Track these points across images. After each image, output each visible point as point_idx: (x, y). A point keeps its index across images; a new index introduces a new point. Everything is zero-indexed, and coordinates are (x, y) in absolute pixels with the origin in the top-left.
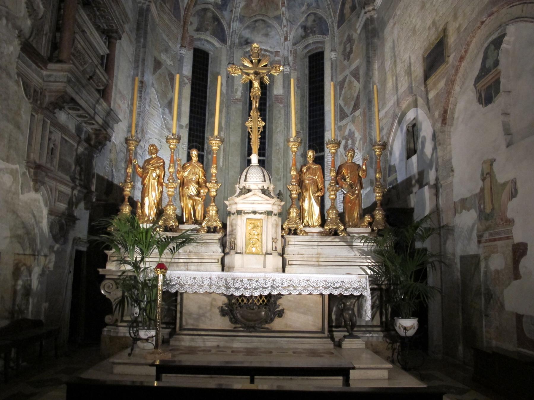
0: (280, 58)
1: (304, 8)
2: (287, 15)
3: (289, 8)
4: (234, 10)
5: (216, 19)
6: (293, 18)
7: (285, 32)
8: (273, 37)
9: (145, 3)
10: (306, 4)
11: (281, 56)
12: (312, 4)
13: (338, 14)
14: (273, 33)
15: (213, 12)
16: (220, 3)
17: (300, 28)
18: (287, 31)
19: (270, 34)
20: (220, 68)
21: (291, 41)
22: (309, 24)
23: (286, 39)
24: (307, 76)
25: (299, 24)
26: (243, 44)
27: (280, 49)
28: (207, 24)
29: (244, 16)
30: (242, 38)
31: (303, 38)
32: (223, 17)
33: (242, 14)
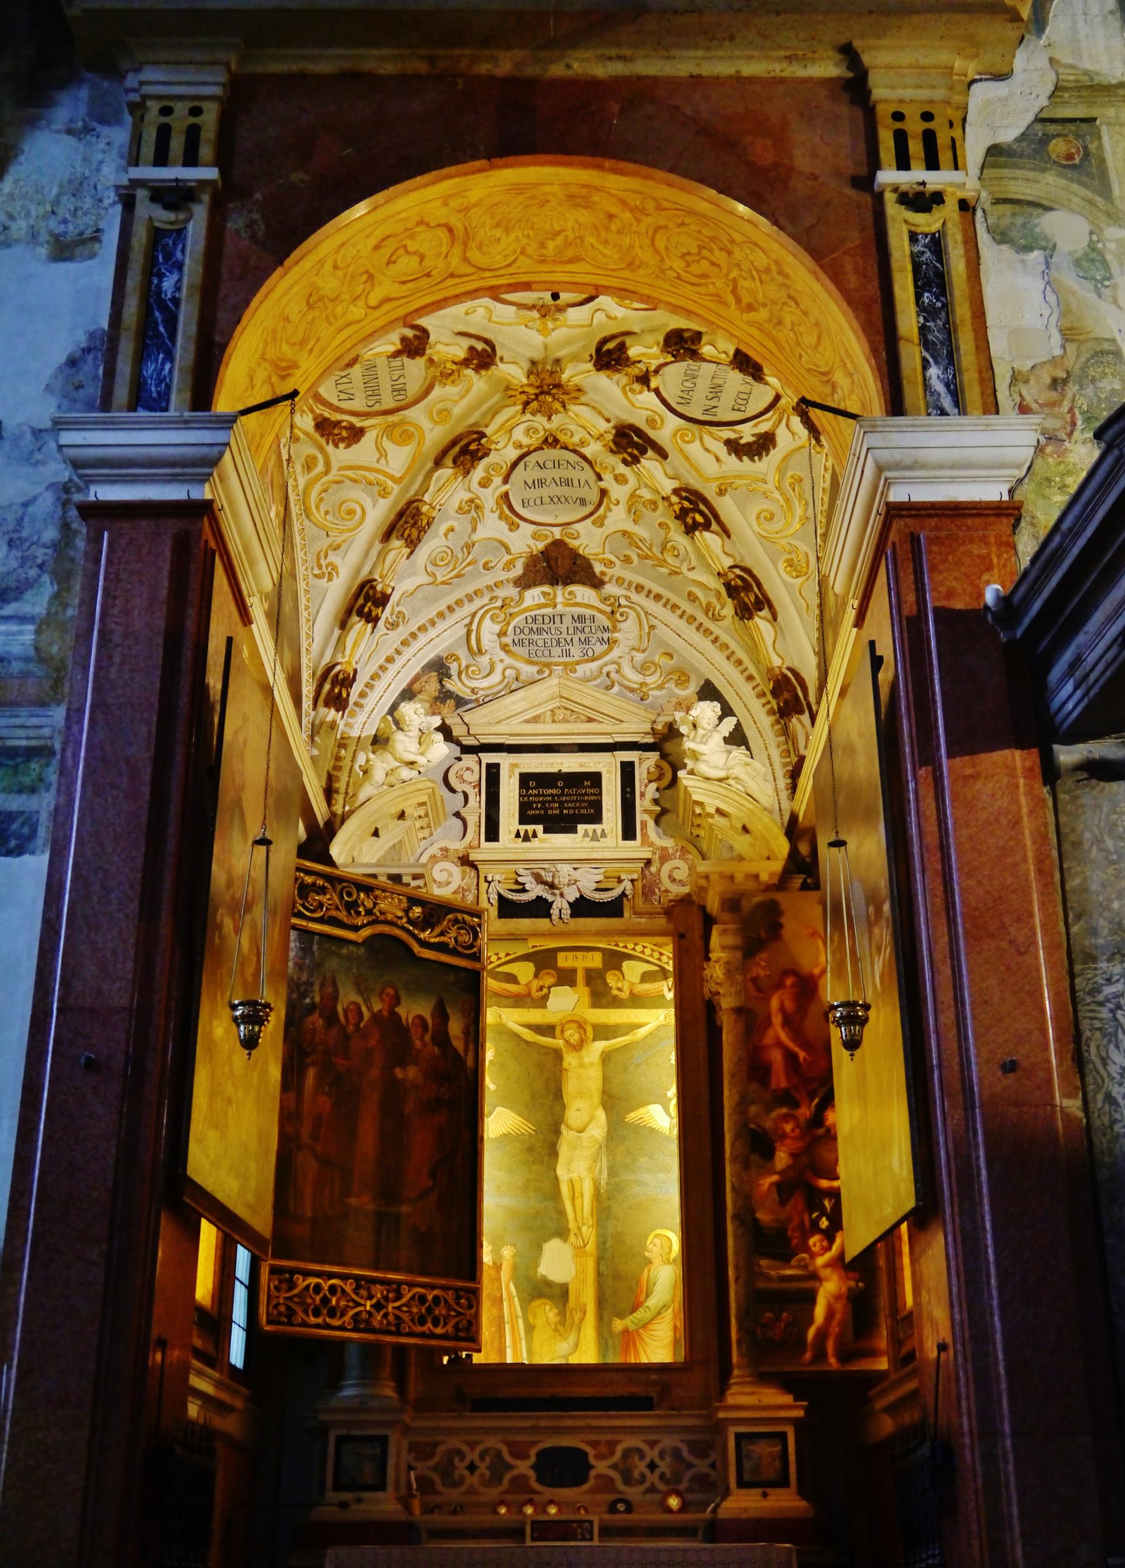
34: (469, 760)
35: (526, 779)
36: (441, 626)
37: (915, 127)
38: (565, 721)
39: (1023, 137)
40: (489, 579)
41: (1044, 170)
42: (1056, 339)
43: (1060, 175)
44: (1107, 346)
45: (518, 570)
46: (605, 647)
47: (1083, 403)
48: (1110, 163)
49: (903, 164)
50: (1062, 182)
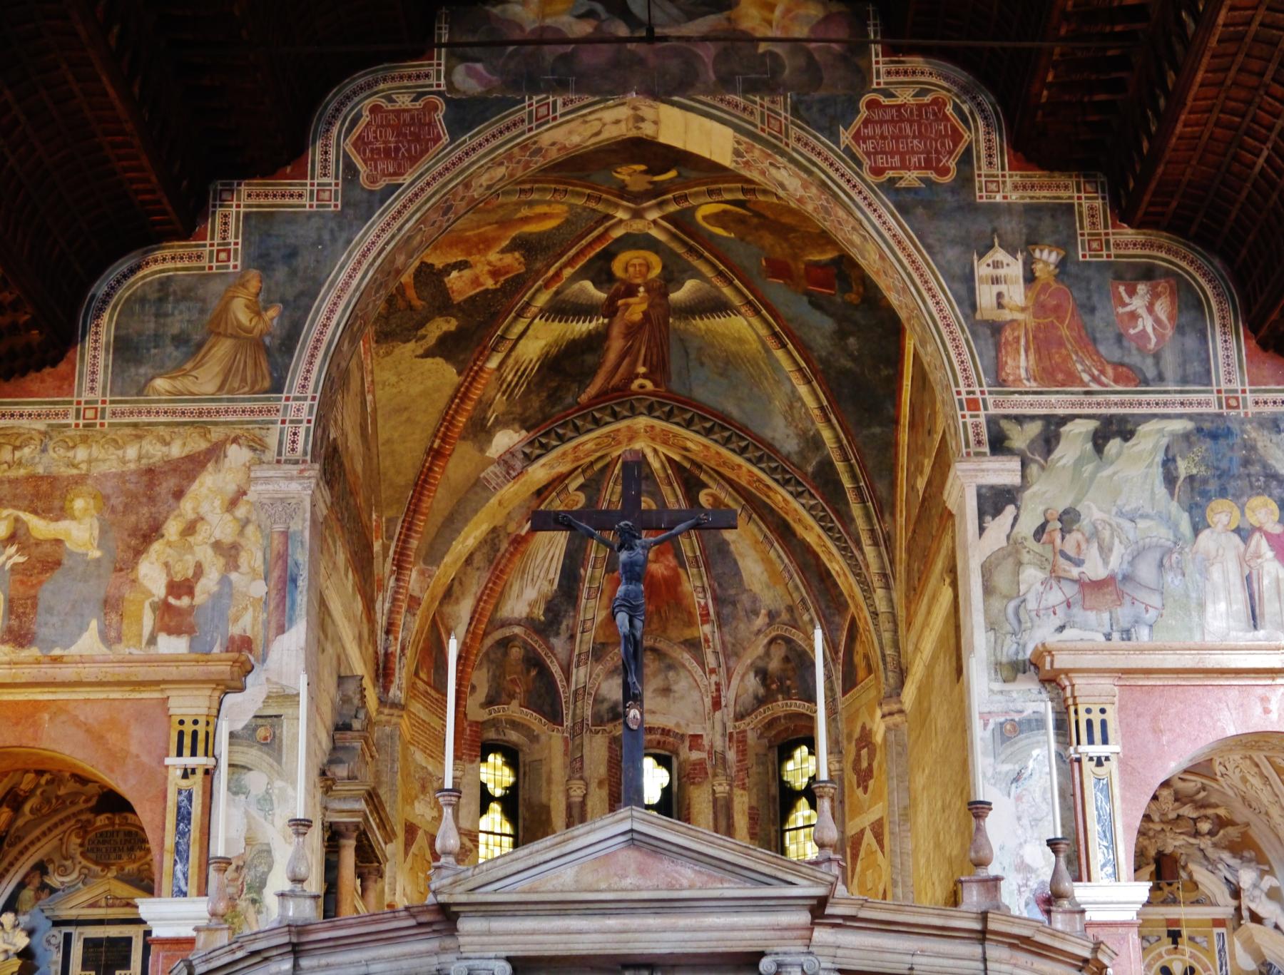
0: (704, 755)
1: (760, 621)
2: (718, 642)
3: (721, 622)
4: (579, 635)
5: (534, 662)
6: (734, 645)
7: (713, 687)
8: (682, 698)
9: (388, 722)
10: (763, 612)
11: (707, 748)
12: (778, 614)
13: (841, 654)
14: (681, 684)
15: (525, 642)
16: (542, 618)
17: (752, 675)
18: (718, 684)
19: (675, 688)
20: (550, 792)
21: (731, 709)
22: (774, 665)
23: (717, 704)
24: (774, 798)
25: (749, 661)
26: (606, 718)
27: (704, 729)
28: (513, 681)
29: (603, 644)
30: (603, 701)
31: (760, 701)
32: (551, 649)
33: (602, 640)
34: (55, 931)
35: (86, 941)
36: (44, 841)
37: (188, 728)
38: (112, 906)
39: (246, 727)
40: (74, 809)
41: (252, 747)
42: (243, 844)
43: (260, 750)
44: (265, 848)
45: (94, 802)
46: (142, 853)
47: (248, 879)
48: (284, 742)
49: (180, 754)
50: (260, 753)
